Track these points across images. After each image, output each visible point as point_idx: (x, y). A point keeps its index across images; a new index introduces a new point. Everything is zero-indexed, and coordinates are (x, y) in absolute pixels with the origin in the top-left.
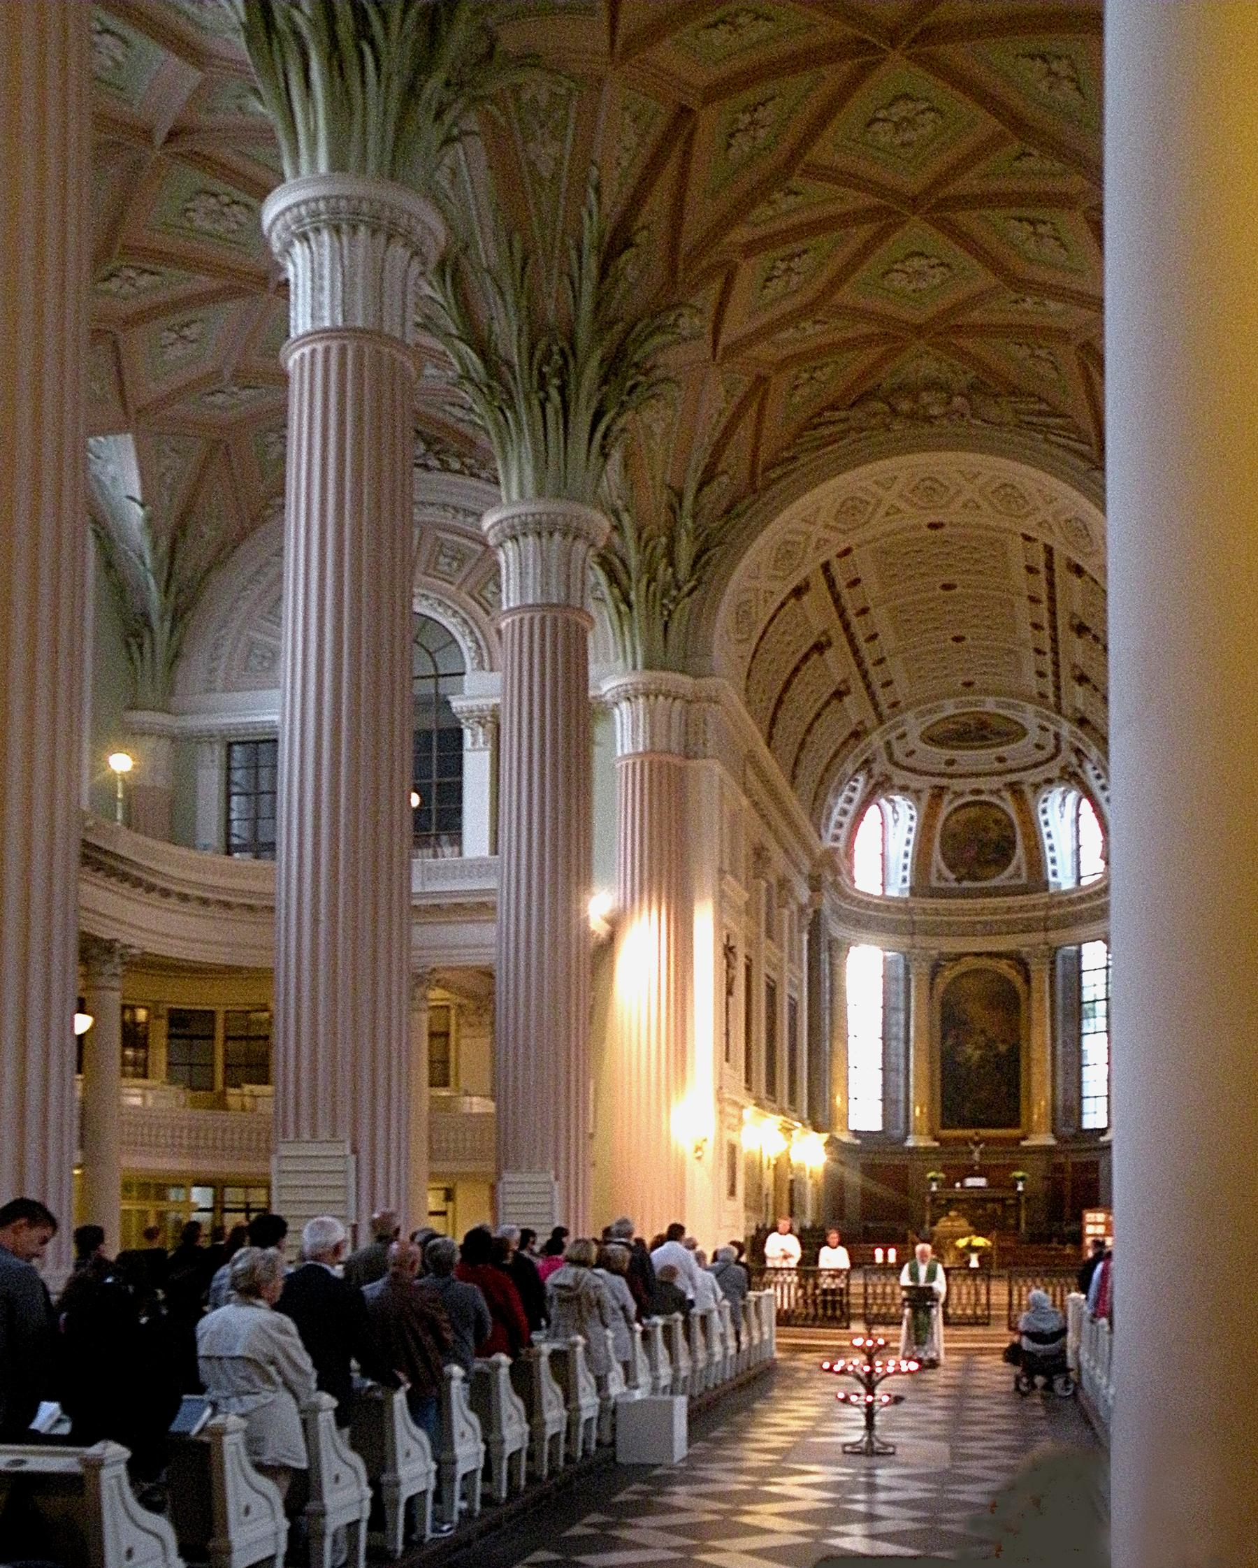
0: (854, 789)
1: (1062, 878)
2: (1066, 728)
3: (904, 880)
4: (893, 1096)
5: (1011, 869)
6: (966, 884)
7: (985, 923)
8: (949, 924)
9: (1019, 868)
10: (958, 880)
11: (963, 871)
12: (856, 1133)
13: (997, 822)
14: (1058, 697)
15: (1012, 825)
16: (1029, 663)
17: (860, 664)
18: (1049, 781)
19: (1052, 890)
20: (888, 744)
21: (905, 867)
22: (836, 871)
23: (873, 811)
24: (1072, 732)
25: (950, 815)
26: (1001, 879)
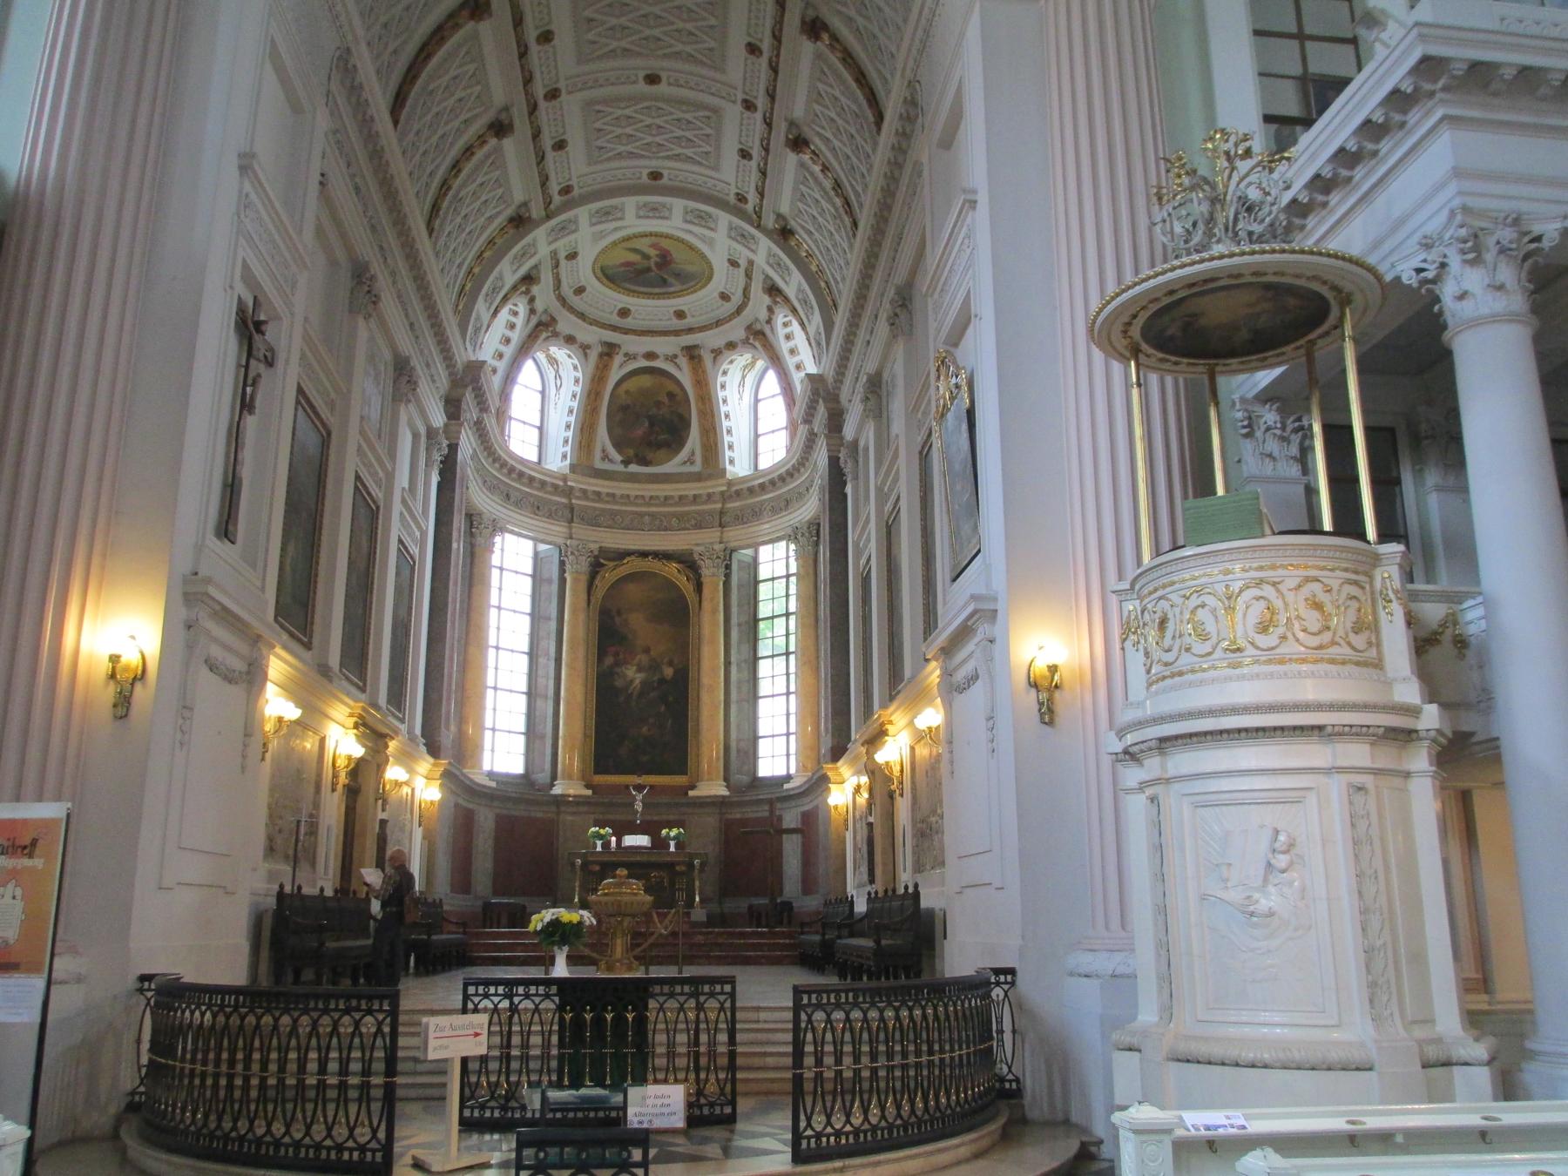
0: (512, 326)
1: (738, 466)
2: (764, 249)
3: (564, 456)
4: (546, 575)
5: (684, 454)
6: (633, 468)
7: (652, 515)
8: (613, 514)
9: (693, 454)
10: (626, 463)
11: (631, 452)
12: (491, 775)
13: (671, 395)
14: (762, 195)
15: (688, 400)
16: (736, 128)
17: (529, 95)
18: (731, 346)
19: (729, 476)
20: (554, 254)
21: (566, 441)
22: (483, 406)
23: (528, 367)
24: (770, 254)
25: (618, 384)
26: (672, 466)
